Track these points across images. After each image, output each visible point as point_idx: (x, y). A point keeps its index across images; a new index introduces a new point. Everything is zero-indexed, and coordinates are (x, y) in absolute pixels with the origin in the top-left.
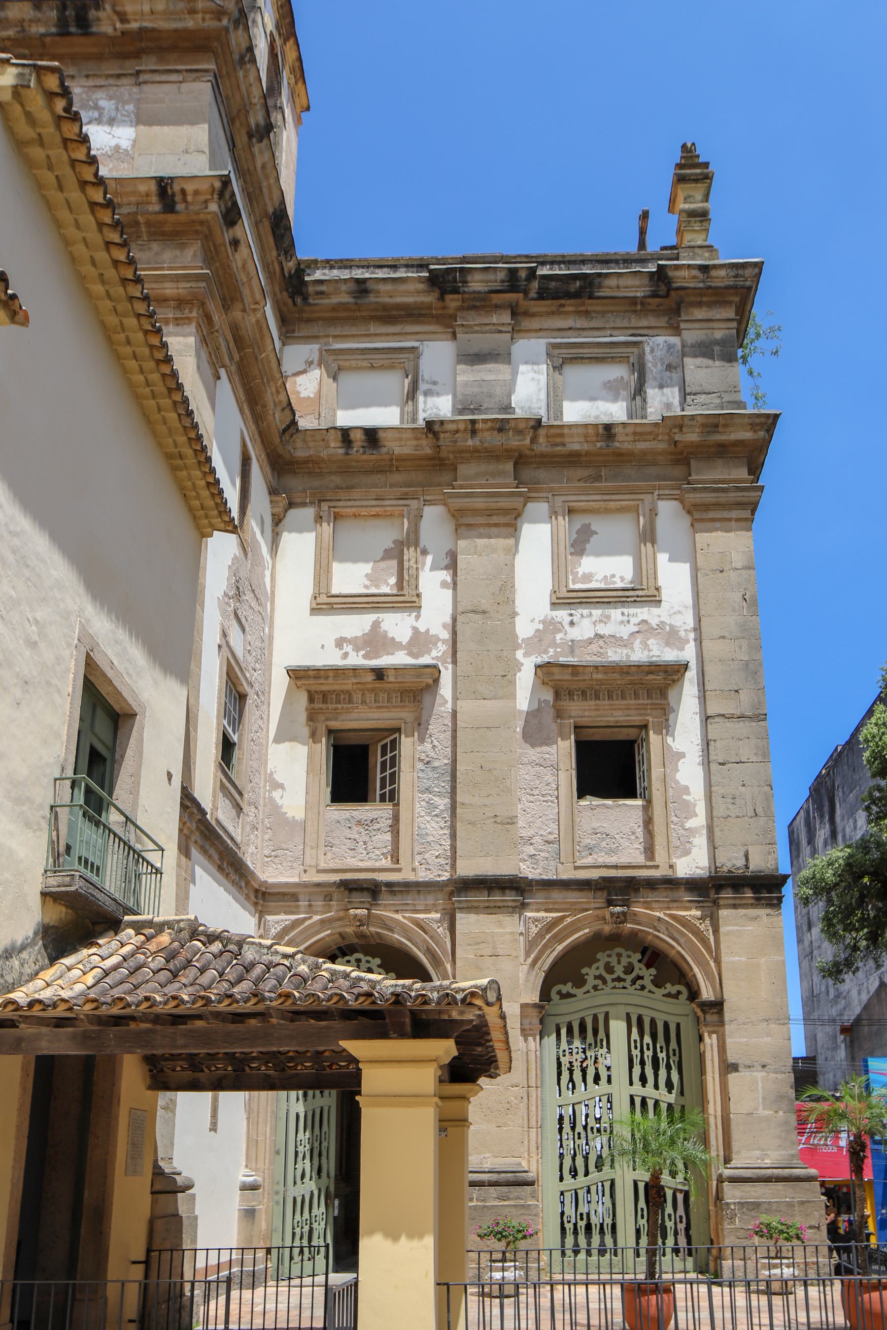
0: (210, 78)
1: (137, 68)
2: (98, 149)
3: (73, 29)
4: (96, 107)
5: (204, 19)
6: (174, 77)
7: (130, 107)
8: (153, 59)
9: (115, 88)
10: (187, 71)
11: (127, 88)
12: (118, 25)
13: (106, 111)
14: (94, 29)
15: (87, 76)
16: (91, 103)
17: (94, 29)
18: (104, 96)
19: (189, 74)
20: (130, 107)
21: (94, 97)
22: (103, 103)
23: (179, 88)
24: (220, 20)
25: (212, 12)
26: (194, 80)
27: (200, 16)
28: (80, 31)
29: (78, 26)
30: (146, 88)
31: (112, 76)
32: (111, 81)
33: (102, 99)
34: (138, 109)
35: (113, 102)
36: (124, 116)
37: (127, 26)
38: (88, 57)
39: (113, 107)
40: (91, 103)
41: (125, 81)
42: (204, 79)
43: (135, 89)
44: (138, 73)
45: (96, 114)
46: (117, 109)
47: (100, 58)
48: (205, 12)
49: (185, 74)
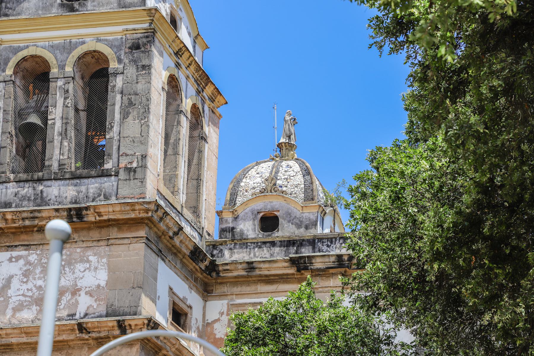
0: (144, 241)
1: (108, 238)
2: (89, 287)
3: (75, 220)
4: (88, 261)
5: (139, 213)
6: (126, 241)
7: (104, 260)
8: (116, 229)
9: (97, 248)
10: (132, 237)
11: (103, 249)
12: (98, 218)
13: (93, 263)
14: (85, 219)
15: (83, 241)
16: (85, 258)
17: (85, 219)
18: (92, 254)
19: (134, 239)
20: (104, 260)
21: (87, 254)
22: (91, 258)
23: (129, 247)
24: (147, 213)
25: (144, 210)
26: (136, 243)
27: (138, 212)
28: (78, 221)
29: (78, 218)
30: (112, 248)
31: (95, 240)
32: (95, 244)
33: (90, 255)
34: (109, 261)
35: (96, 257)
36: (102, 266)
37: (101, 218)
38: (83, 229)
39: (96, 260)
40: (85, 258)
41: (102, 243)
42: (141, 242)
43: (107, 248)
44: (108, 239)
45: (88, 266)
46: (98, 262)
47: (89, 229)
48: (140, 210)
49: (131, 239)
